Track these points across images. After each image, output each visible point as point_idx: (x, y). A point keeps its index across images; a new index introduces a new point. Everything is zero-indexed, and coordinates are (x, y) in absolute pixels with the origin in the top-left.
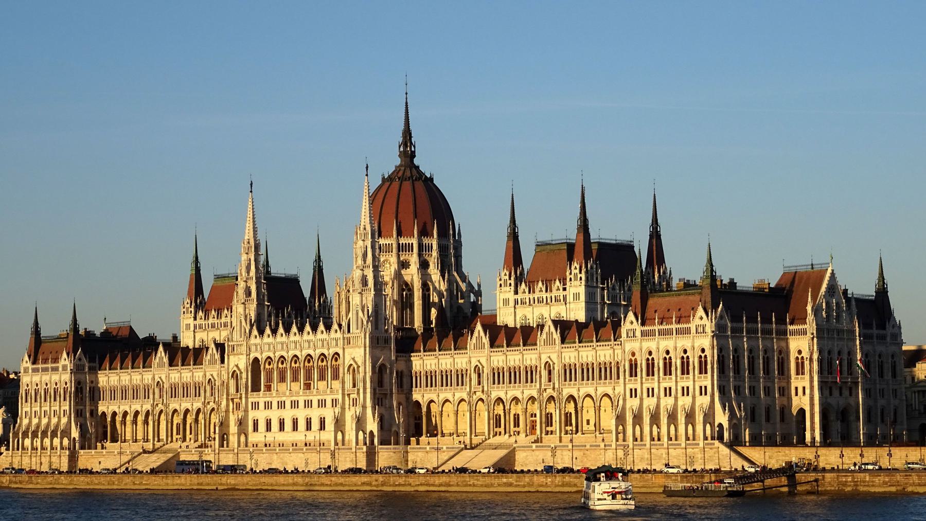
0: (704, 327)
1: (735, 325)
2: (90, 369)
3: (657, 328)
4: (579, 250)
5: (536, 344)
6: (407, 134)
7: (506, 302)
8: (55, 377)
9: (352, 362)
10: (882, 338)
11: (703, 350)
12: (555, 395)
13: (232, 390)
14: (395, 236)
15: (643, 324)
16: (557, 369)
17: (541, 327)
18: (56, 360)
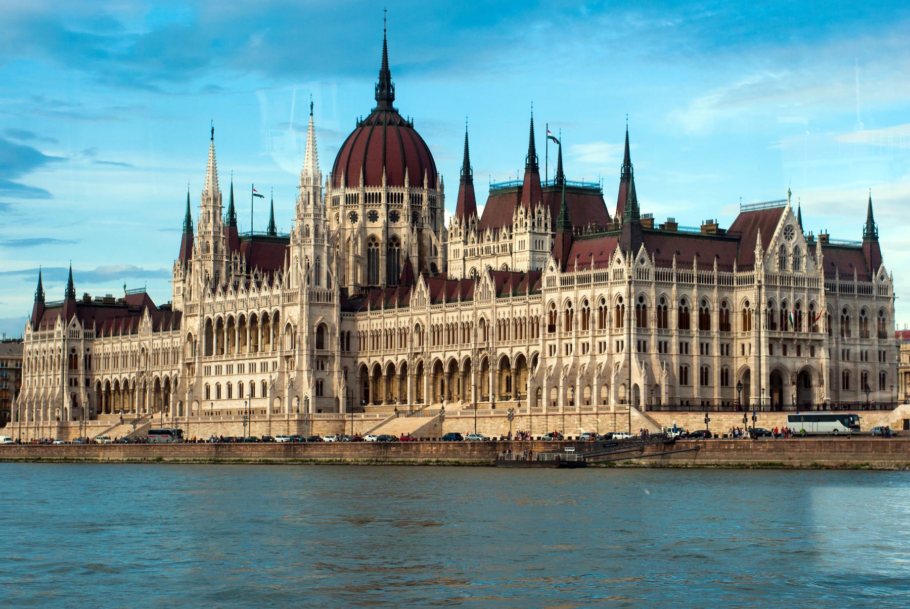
0: (622, 271)
1: (660, 270)
2: (86, 335)
3: (576, 274)
4: (526, 193)
7: (456, 252)
8: (51, 345)
9: (289, 321)
10: (869, 290)
11: (621, 299)
12: (489, 355)
14: (361, 185)
15: (564, 270)
16: (493, 324)
17: (476, 278)
18: (52, 327)
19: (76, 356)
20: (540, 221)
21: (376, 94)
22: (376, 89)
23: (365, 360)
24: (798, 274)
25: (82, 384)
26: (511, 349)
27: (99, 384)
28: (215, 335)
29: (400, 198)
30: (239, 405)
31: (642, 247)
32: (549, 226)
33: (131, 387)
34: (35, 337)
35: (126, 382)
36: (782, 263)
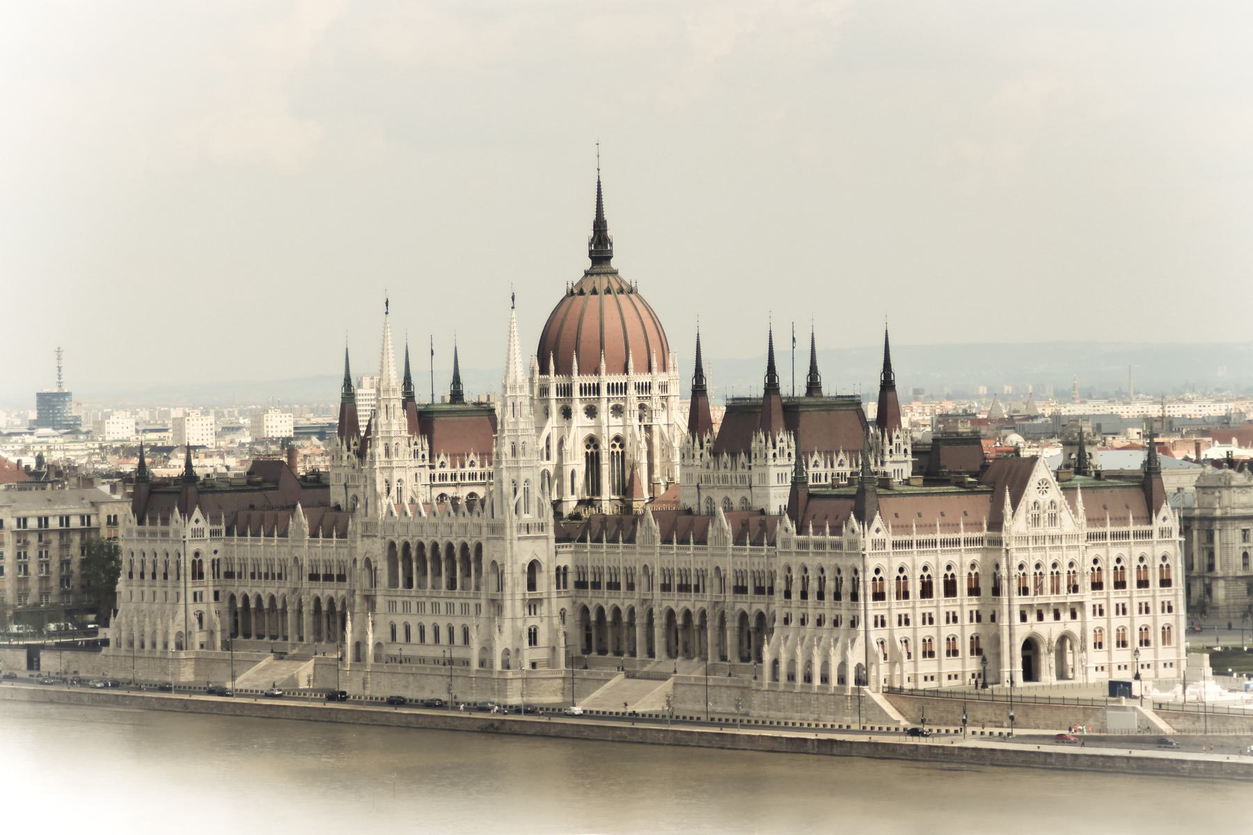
2: (212, 533)
5: (705, 543)
6: (600, 226)
8: (165, 546)
15: (798, 533)
18: (165, 521)
19: (200, 561)
20: (782, 451)
21: (591, 252)
22: (590, 245)
23: (586, 602)
24: (1054, 531)
25: (209, 595)
26: (752, 605)
27: (233, 598)
28: (400, 564)
29: (623, 388)
30: (437, 652)
31: (878, 516)
32: (793, 455)
33: (279, 606)
34: (141, 534)
35: (272, 599)
36: (1036, 520)
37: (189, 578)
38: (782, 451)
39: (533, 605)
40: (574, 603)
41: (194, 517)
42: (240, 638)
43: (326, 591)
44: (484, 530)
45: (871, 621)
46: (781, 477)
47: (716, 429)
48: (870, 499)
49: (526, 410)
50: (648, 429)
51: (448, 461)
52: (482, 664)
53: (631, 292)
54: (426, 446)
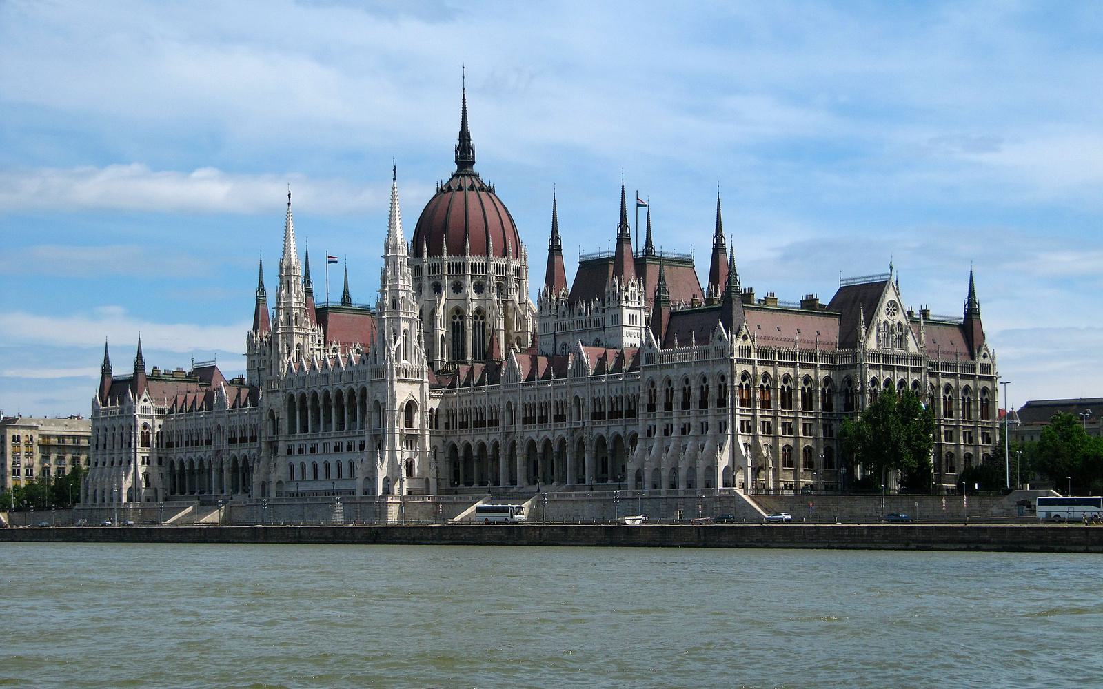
13: (270, 432)
20: (633, 294)
23: (455, 440)
26: (610, 429)
27: (172, 463)
28: (298, 413)
29: (485, 268)
33: (206, 467)
35: (201, 461)
37: (139, 446)
38: (633, 294)
39: (410, 440)
40: (444, 442)
41: (144, 396)
42: (177, 494)
43: (240, 451)
44: (369, 374)
45: (738, 425)
46: (633, 318)
47: (570, 286)
48: (737, 307)
49: (405, 269)
50: (505, 303)
51: (339, 347)
52: (366, 492)
53: (490, 191)
54: (322, 334)
